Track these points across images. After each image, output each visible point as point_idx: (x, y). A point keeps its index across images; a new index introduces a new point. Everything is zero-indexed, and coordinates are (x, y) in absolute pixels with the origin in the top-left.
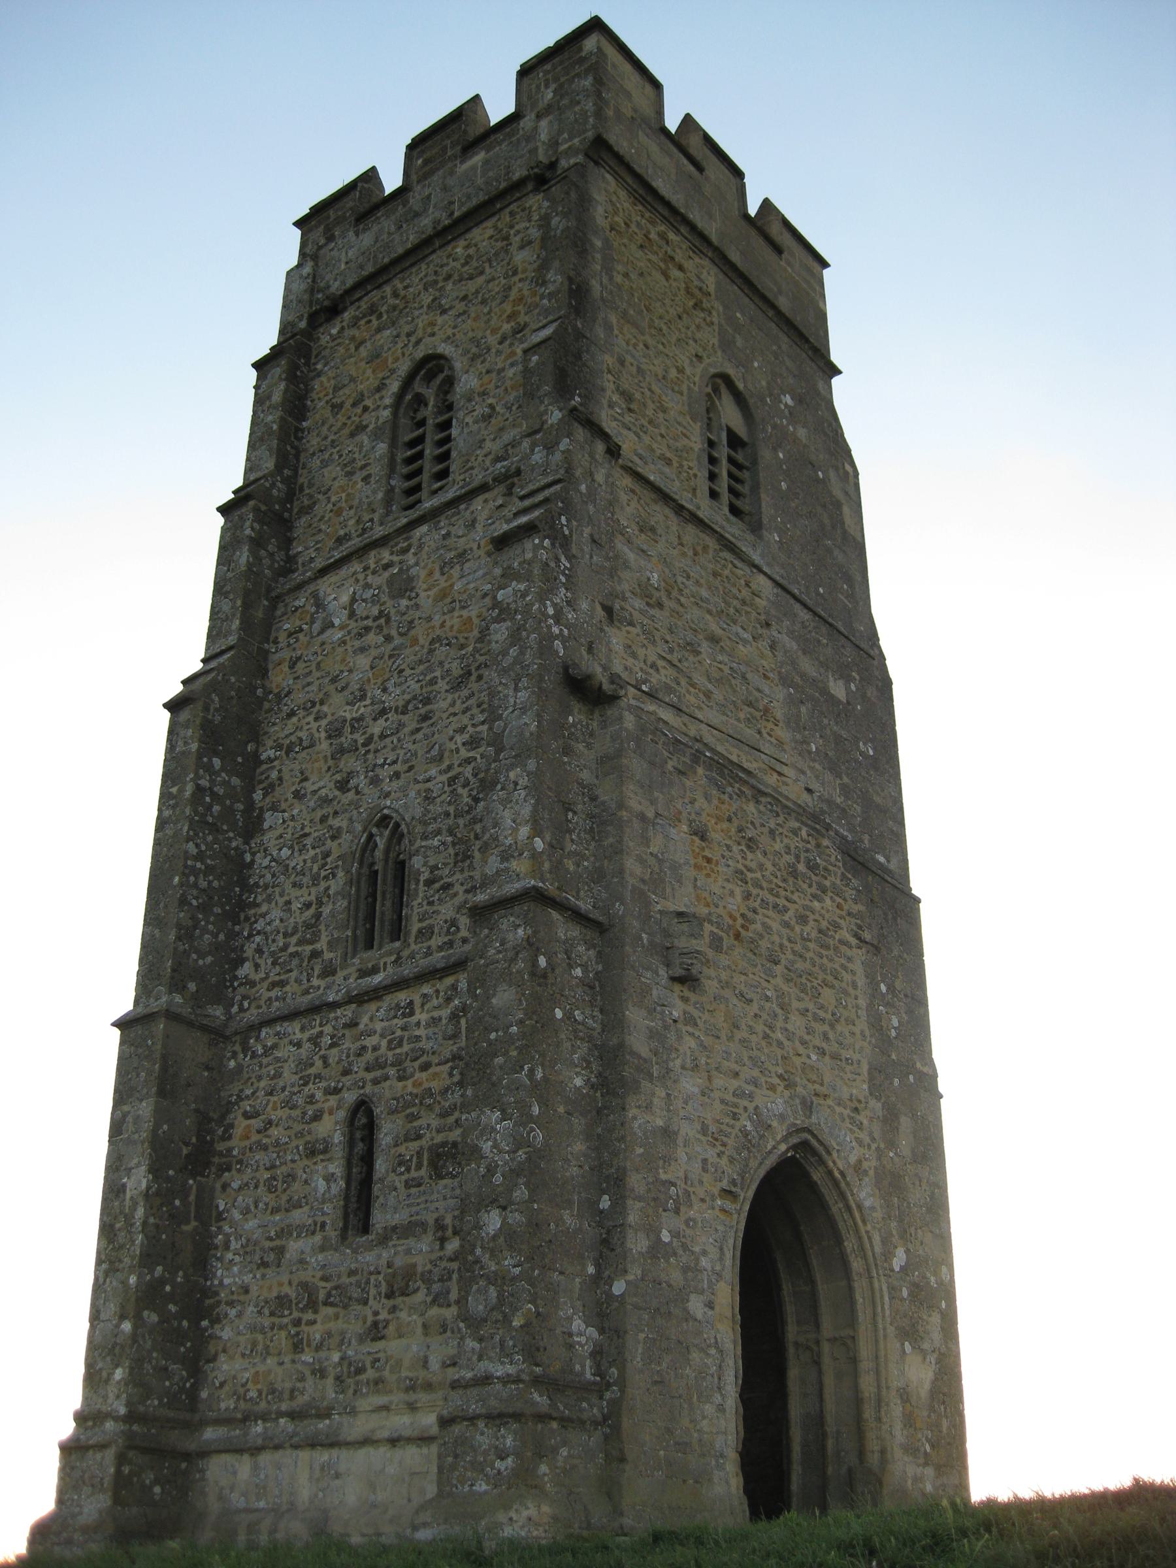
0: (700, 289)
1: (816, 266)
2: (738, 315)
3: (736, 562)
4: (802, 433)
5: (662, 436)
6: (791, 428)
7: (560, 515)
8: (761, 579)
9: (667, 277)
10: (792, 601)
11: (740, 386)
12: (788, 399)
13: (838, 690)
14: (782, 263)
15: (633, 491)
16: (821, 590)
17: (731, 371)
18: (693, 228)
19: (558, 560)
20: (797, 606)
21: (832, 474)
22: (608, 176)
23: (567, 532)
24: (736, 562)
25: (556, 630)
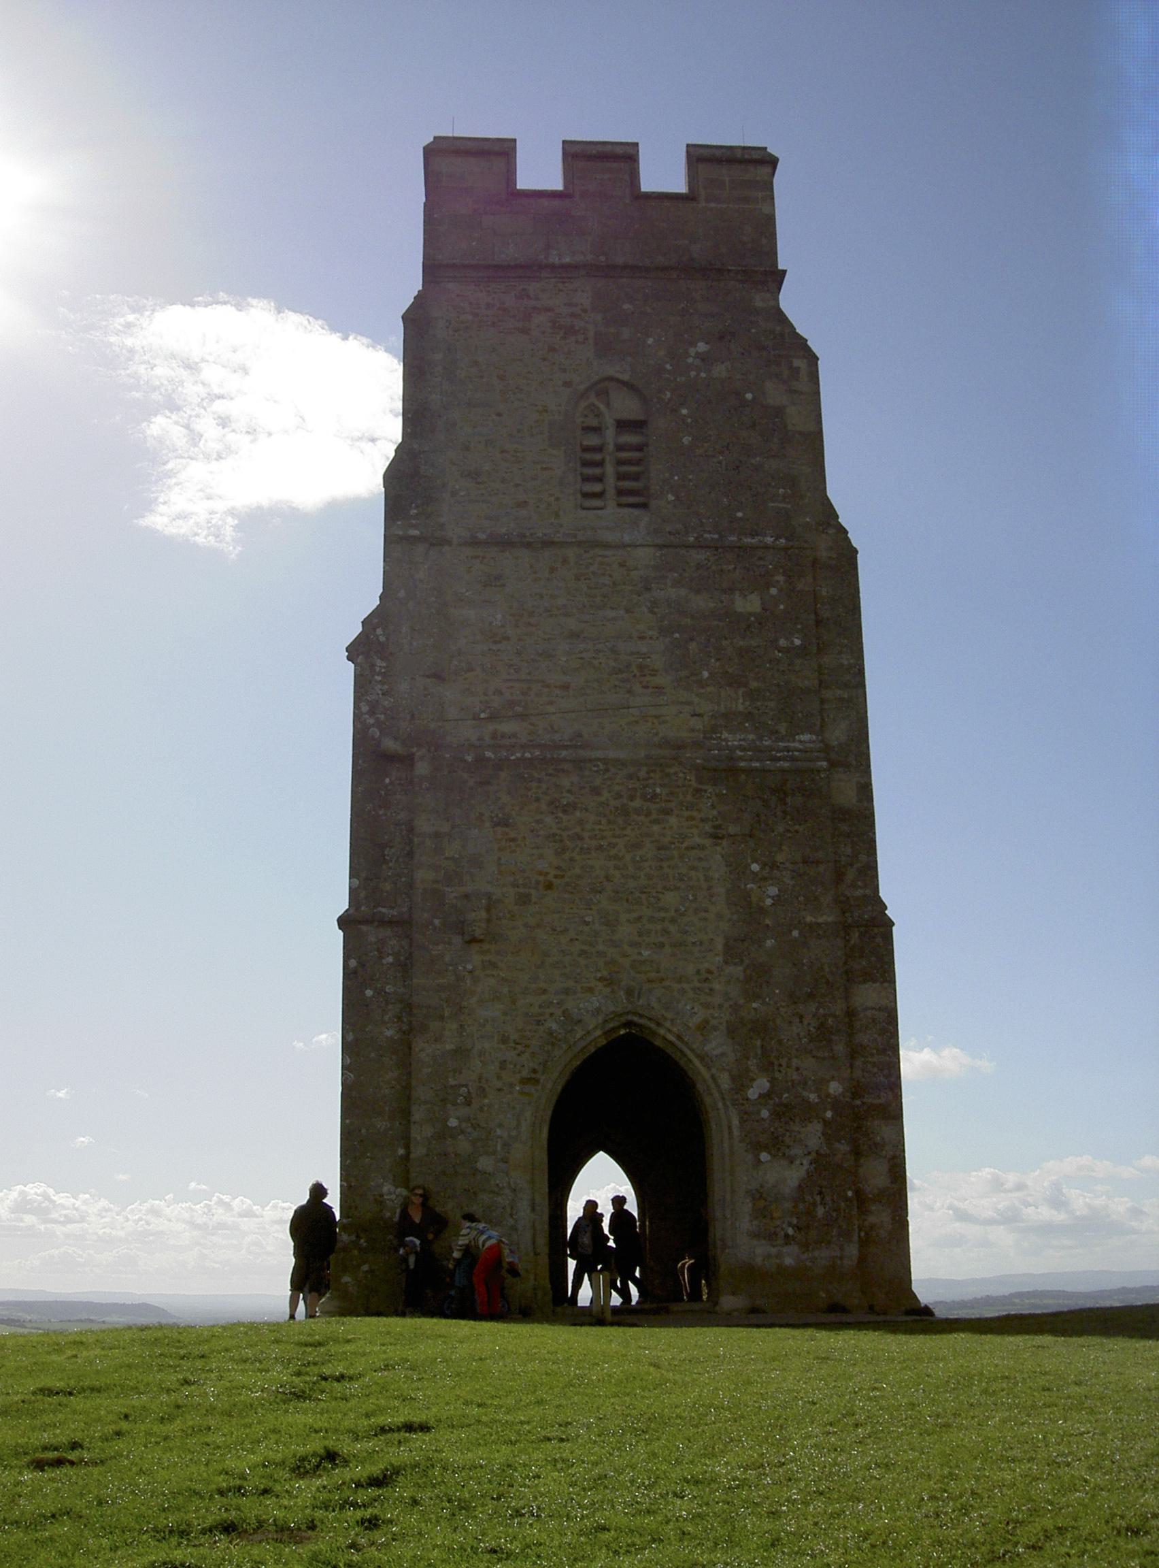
0: (573, 315)
1: (766, 170)
2: (626, 306)
3: (606, 553)
4: (720, 370)
5: (517, 485)
6: (703, 375)
7: (375, 630)
8: (640, 552)
9: (525, 331)
10: (683, 552)
11: (625, 377)
12: (702, 347)
13: (750, 604)
14: (703, 204)
15: (476, 557)
16: (740, 514)
17: (611, 371)
18: (553, 267)
19: (373, 666)
20: (693, 552)
21: (769, 386)
22: (450, 286)
23: (382, 639)
24: (606, 553)
25: (372, 721)
